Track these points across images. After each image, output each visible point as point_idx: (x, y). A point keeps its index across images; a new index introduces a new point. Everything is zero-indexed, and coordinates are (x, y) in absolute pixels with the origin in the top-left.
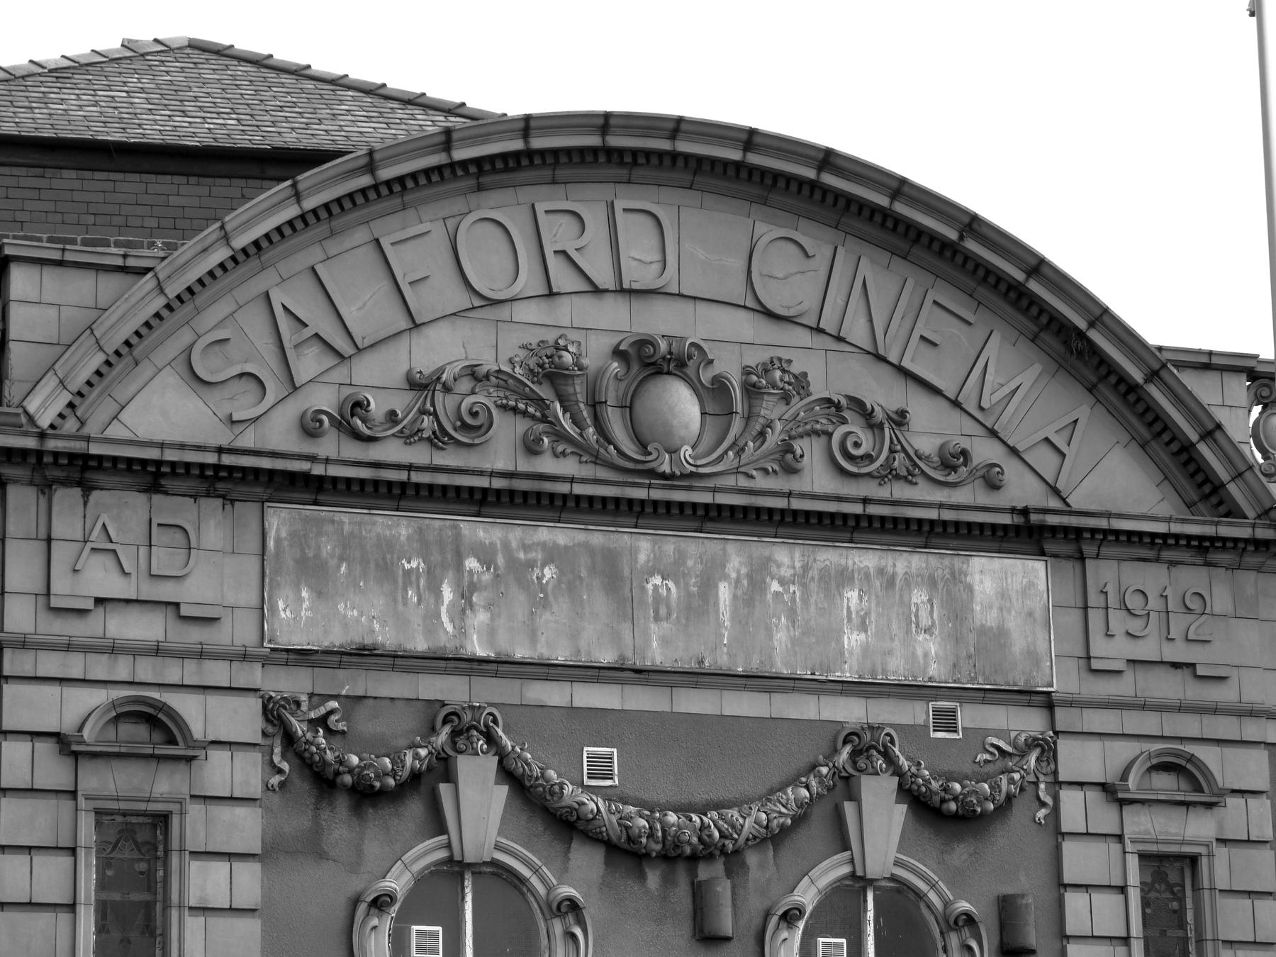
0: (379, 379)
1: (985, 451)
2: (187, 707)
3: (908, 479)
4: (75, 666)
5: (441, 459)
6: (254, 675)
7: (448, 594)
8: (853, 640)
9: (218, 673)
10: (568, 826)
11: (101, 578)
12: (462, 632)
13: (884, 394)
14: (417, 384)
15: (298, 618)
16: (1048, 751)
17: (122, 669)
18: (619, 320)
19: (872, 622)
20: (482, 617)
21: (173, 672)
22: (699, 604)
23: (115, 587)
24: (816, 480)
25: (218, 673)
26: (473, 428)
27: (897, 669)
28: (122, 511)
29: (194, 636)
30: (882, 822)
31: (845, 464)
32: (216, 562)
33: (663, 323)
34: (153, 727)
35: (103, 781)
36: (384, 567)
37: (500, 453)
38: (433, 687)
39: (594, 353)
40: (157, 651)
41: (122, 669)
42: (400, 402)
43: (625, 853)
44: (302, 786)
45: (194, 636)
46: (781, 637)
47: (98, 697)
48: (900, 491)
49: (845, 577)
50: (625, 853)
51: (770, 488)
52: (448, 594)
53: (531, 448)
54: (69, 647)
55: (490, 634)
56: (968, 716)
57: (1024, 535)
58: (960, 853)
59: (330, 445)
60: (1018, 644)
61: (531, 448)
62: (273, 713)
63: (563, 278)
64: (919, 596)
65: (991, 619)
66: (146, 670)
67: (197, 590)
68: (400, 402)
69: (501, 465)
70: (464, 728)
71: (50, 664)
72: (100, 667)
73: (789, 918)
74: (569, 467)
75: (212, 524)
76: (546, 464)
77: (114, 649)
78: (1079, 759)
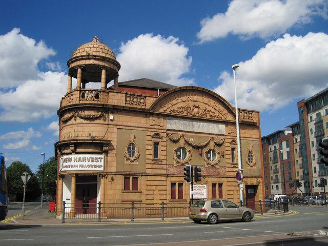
4: (152, 130)
9: (163, 131)
10: (190, 145)
11: (154, 123)
15: (169, 127)
17: (156, 130)
25: (163, 131)
26: (182, 112)
29: (161, 128)
33: (197, 104)
40: (158, 129)
41: (156, 130)
43: (194, 147)
45: (162, 128)
47: (154, 133)
50: (194, 147)
61: (187, 114)
66: (158, 131)
67: (161, 125)
71: (150, 130)
72: (154, 130)
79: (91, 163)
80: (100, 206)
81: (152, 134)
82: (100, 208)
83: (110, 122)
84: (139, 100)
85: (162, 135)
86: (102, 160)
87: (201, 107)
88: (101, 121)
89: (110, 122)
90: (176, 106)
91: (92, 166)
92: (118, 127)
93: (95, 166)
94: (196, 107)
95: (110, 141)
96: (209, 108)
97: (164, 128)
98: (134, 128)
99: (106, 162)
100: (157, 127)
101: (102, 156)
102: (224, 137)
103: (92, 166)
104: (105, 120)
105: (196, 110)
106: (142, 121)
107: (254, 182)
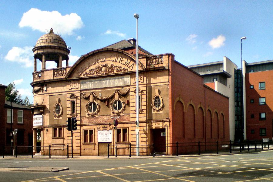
7: (91, 84)
11: (72, 87)
12: (91, 87)
20: (93, 86)
22: (106, 83)
29: (76, 90)
40: (74, 91)
41: (72, 92)
45: (78, 90)
46: (111, 84)
47: (71, 94)
52: (91, 84)
55: (93, 87)
60: (127, 82)
81: (69, 95)
101: (41, 116)
102: (129, 88)
104: (43, 92)
107: (160, 126)
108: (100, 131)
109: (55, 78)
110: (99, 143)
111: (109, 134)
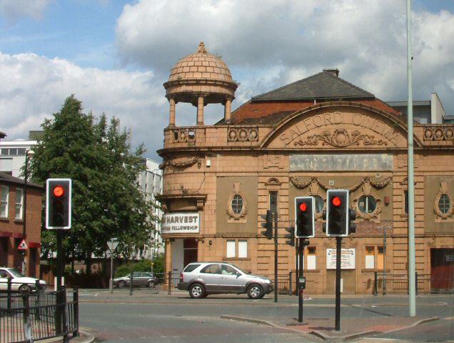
0: (304, 138)
1: (384, 140)
2: (279, 179)
3: (374, 144)
4: (267, 174)
5: (311, 147)
6: (287, 174)
8: (365, 166)
9: (283, 174)
11: (270, 164)
13: (372, 134)
14: (308, 138)
15: (293, 167)
16: (391, 178)
17: (272, 174)
18: (335, 127)
19: (368, 163)
21: (278, 174)
23: (271, 165)
24: (362, 145)
25: (283, 174)
26: (315, 143)
27: (370, 169)
28: (272, 157)
30: (368, 189)
31: (366, 143)
32: (284, 161)
33: (340, 127)
34: (274, 180)
35: (269, 187)
36: (303, 161)
37: (320, 145)
38: (310, 174)
39: (332, 133)
40: (276, 172)
41: (272, 174)
42: (306, 140)
44: (293, 187)
47: (269, 178)
48: (373, 146)
49: (364, 158)
51: (354, 147)
53: (323, 145)
54: (266, 172)
56: (380, 174)
57: (388, 151)
58: (379, 191)
59: (298, 146)
61: (323, 145)
62: (290, 178)
63: (328, 123)
64: (374, 160)
65: (384, 162)
67: (280, 165)
68: (306, 140)
69: (320, 147)
70: (314, 179)
71: (263, 174)
72: (269, 174)
73: (355, 201)
74: (328, 146)
75: (282, 157)
76: (325, 146)
77: (271, 172)
78: (395, 179)
79: (184, 224)
80: (170, 276)
81: (266, 179)
82: (170, 279)
83: (208, 170)
84: (238, 134)
85: (280, 180)
86: (198, 219)
87: (350, 132)
88: (194, 168)
89: (208, 170)
90: (306, 135)
91: (185, 228)
92: (218, 175)
93: (188, 228)
94: (339, 133)
95: (206, 195)
96: (363, 132)
97: (287, 170)
98: (241, 174)
99: (202, 221)
100: (275, 169)
102: (390, 174)
103: (185, 228)
105: (341, 137)
106: (248, 163)
108: (331, 249)
109: (231, 144)
110: (328, 270)
111: (350, 255)
